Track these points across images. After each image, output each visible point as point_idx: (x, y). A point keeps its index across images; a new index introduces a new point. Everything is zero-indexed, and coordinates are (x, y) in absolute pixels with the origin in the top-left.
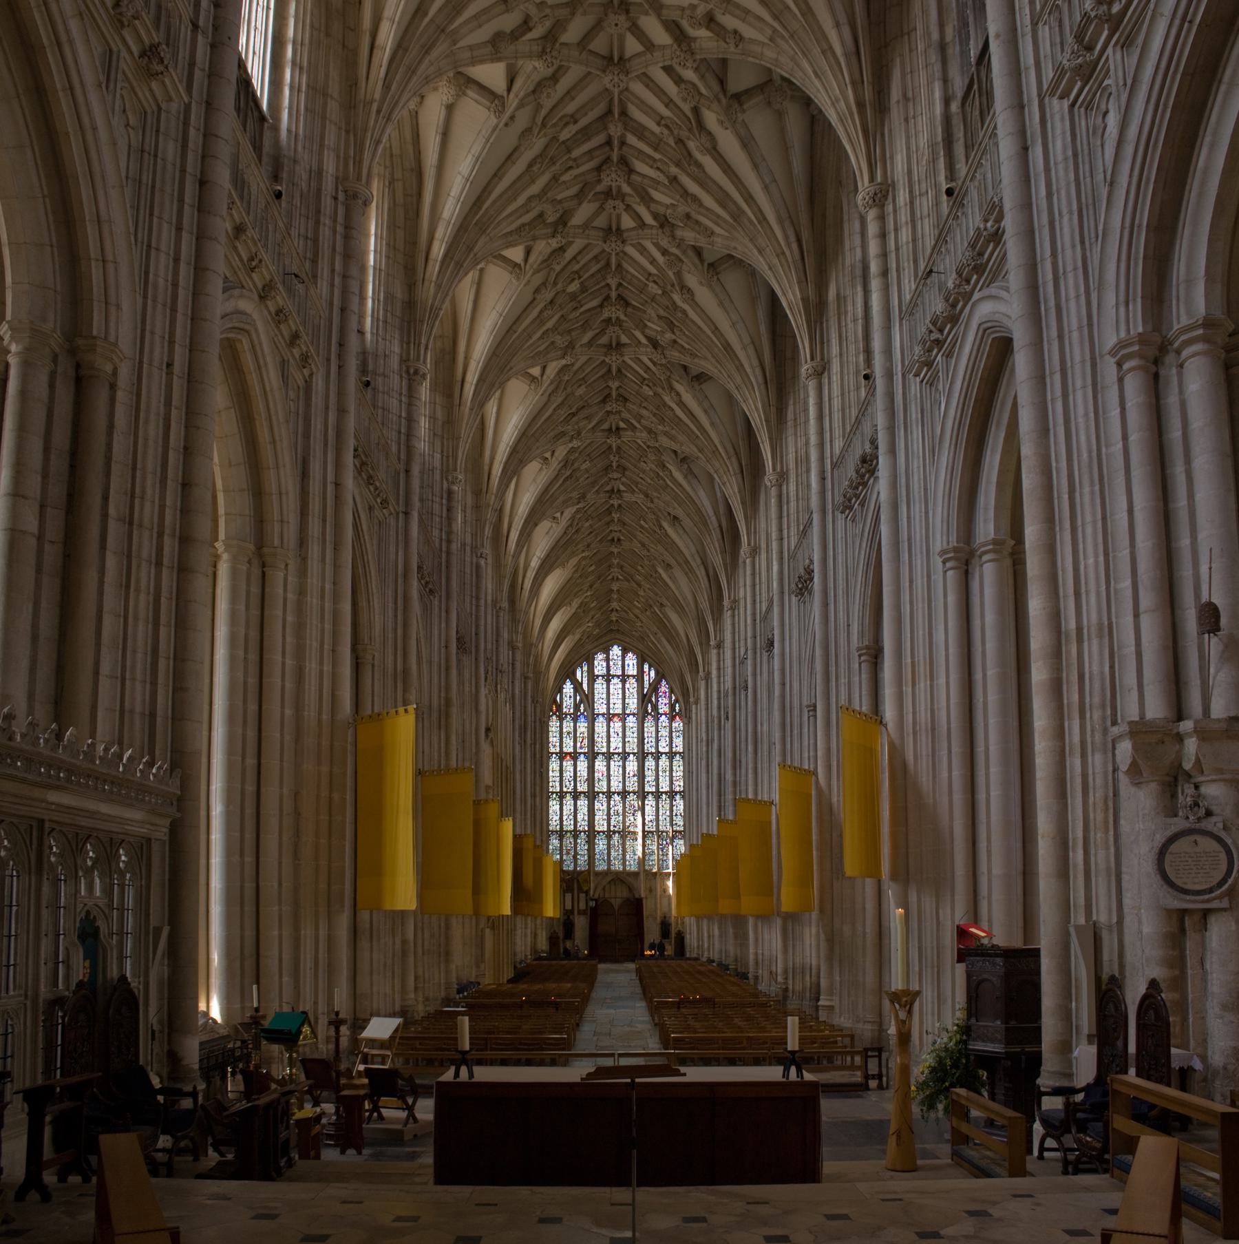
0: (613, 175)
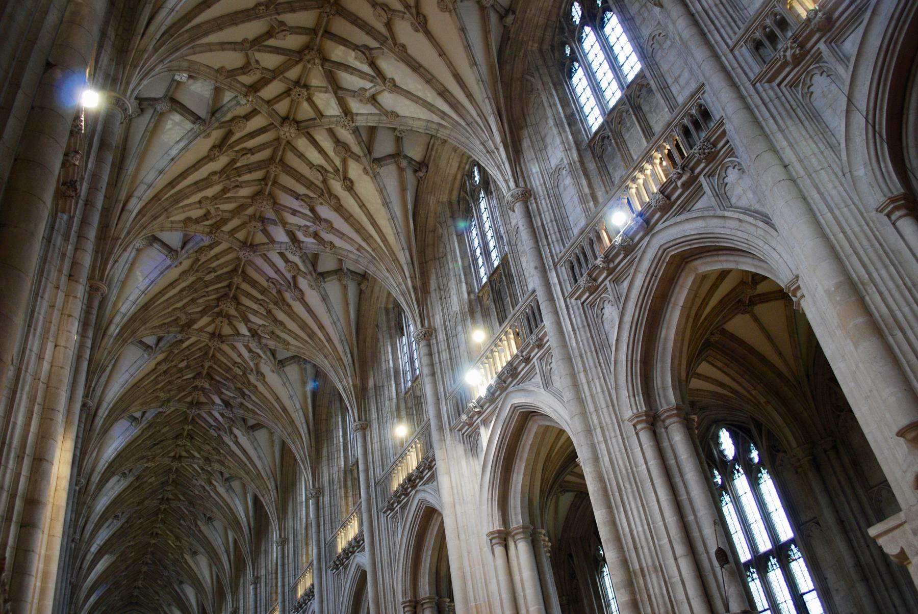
0: (229, 304)
